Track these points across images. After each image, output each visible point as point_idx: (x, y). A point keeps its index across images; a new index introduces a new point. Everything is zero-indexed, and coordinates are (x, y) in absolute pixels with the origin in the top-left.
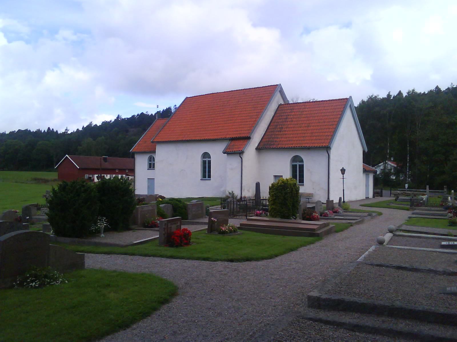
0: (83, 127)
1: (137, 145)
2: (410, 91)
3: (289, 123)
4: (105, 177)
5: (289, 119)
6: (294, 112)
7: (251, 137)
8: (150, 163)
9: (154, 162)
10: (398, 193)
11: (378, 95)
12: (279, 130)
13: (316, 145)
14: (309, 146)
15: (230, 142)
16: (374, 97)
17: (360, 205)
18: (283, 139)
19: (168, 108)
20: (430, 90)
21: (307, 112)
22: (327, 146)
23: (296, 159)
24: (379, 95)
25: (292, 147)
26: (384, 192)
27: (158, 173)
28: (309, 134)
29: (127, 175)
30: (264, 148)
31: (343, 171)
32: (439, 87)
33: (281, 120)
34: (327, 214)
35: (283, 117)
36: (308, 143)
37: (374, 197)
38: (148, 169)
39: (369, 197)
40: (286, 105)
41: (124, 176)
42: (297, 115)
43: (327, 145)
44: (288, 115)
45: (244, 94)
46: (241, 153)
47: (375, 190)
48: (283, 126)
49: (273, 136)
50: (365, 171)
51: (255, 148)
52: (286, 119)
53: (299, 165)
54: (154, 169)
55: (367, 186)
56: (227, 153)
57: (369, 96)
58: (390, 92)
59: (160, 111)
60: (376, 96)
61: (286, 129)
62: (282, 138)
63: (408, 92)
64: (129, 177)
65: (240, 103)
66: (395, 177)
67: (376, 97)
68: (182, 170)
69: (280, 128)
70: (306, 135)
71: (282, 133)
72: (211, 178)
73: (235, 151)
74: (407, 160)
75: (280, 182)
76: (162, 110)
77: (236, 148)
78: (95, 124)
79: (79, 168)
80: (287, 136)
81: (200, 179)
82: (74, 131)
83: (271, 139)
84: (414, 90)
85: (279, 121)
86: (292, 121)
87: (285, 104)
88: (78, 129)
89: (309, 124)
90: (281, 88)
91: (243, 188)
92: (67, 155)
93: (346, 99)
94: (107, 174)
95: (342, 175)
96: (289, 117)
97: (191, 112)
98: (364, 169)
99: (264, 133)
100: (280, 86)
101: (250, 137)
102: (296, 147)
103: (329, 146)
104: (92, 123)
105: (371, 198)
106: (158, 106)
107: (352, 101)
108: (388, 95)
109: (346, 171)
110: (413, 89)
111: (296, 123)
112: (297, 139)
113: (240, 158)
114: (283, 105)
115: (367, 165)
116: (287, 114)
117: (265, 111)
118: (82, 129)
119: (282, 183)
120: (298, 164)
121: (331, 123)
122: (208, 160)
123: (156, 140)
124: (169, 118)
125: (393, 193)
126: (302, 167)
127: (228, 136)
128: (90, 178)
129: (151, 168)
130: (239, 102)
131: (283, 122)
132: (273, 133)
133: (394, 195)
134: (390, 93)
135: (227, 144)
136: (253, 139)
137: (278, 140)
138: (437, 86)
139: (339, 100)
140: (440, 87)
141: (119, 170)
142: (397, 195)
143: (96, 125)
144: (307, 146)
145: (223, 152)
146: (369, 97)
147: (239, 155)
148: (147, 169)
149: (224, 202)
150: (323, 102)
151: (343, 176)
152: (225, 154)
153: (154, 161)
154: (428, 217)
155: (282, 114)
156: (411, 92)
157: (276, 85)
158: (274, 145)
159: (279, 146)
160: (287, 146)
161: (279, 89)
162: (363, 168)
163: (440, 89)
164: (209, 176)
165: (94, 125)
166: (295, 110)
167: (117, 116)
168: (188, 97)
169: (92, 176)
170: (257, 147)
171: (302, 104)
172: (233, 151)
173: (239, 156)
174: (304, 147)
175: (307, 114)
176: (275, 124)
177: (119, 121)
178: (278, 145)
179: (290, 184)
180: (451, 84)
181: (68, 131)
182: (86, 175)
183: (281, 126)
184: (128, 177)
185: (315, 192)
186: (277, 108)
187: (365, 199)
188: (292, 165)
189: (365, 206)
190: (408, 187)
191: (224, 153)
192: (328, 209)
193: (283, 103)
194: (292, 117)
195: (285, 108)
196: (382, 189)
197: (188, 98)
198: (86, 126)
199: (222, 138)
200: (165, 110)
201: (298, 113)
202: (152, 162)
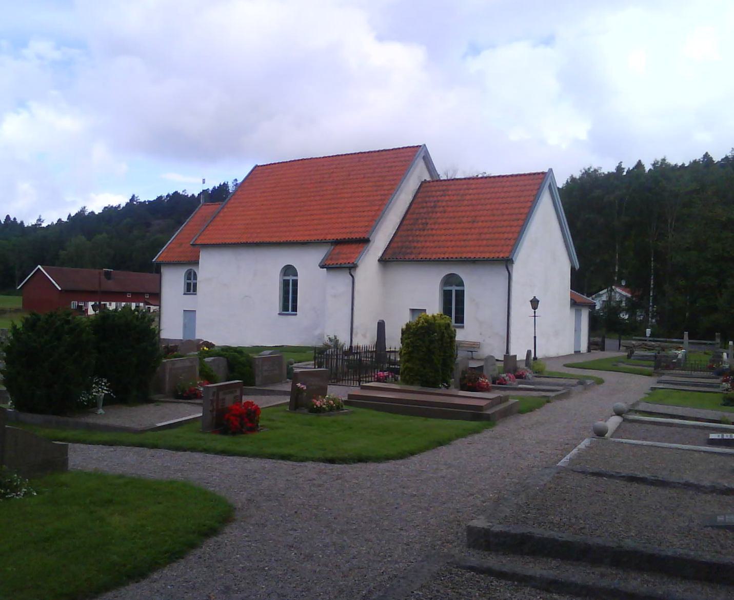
0: (70, 215)
1: (166, 250)
2: (658, 162)
3: (439, 215)
4: (108, 306)
5: (440, 207)
6: (449, 196)
7: (370, 239)
8: (188, 283)
9: (195, 281)
10: (633, 344)
12: (421, 226)
13: (487, 256)
14: (475, 258)
15: (333, 247)
16: (592, 172)
17: (565, 365)
18: (428, 244)
19: (222, 184)
20: (694, 159)
21: (472, 197)
22: (507, 257)
23: (450, 280)
24: (601, 168)
25: (443, 258)
26: (607, 341)
27: (201, 301)
28: (474, 236)
29: (146, 303)
30: (393, 259)
31: (535, 303)
32: (709, 155)
33: (425, 210)
34: (505, 380)
35: (429, 204)
36: (472, 252)
37: (589, 350)
38: (184, 294)
39: (580, 351)
40: (435, 183)
41: (142, 304)
42: (454, 201)
43: (506, 255)
44: (438, 201)
45: (359, 161)
46: (351, 268)
47: (592, 339)
48: (428, 220)
49: (411, 238)
50: (574, 304)
51: (378, 259)
52: (435, 207)
53: (456, 290)
54: (196, 294)
55: (577, 330)
56: (326, 266)
57: (584, 169)
58: (621, 162)
59: (208, 189)
61: (433, 226)
62: (426, 241)
64: (151, 306)
65: (351, 177)
66: (627, 315)
67: (596, 171)
68: (247, 296)
69: (423, 224)
70: (469, 237)
71: (425, 232)
72: (297, 311)
73: (341, 264)
74: (650, 286)
75: (421, 322)
76: (211, 188)
77: (343, 259)
78: (90, 211)
79: (60, 289)
80: (435, 238)
81: (278, 313)
82: (53, 223)
83: (407, 243)
84: (664, 160)
85: (421, 210)
86: (445, 212)
87: (433, 181)
88: (60, 220)
89: (476, 217)
90: (427, 152)
91: (354, 331)
92: (39, 266)
93: (543, 173)
94: (111, 301)
95: (533, 310)
96: (440, 204)
97: (264, 192)
98: (572, 301)
99: (394, 232)
100: (424, 149)
101: (369, 238)
102: (452, 258)
103: (510, 257)
104: (86, 208)
105: (584, 352)
106: (204, 180)
107: (553, 178)
108: (618, 167)
109: (540, 303)
110: (663, 158)
111: (451, 215)
112: (453, 243)
113: (350, 276)
114: (429, 182)
115: (577, 293)
116: (435, 199)
117: (396, 193)
118: (68, 219)
119: (425, 322)
120: (454, 289)
121: (514, 217)
122: (292, 280)
123: (199, 242)
124: (224, 203)
126: (460, 295)
127: (329, 237)
128: (80, 307)
129: (190, 291)
130: (349, 175)
131: (428, 213)
132: (409, 233)
133: (625, 348)
134: (622, 164)
135: (327, 253)
136: (374, 242)
137: (419, 245)
138: (707, 153)
139: (530, 174)
140: (711, 156)
141: (133, 294)
142: (631, 347)
143: (92, 213)
144: (470, 258)
145: (319, 266)
146: (583, 171)
147: (348, 271)
148: (183, 293)
149: (320, 355)
150: (501, 179)
151: (535, 312)
152: (323, 268)
153: (196, 280)
154: (686, 388)
155: (427, 199)
156: (659, 163)
157: (417, 146)
158: (411, 253)
159: (421, 256)
160: (434, 256)
161: (422, 154)
162: (571, 299)
163: (711, 158)
164: (295, 309)
165: (89, 213)
166: (450, 193)
167: (130, 198)
168: (259, 165)
169: (83, 305)
170: (381, 257)
171: (464, 181)
172: (337, 264)
173: (349, 274)
174: (466, 259)
175: (472, 200)
176: (415, 216)
177: (134, 207)
178: (419, 254)
179: (440, 326)
180: (731, 149)
181: (42, 222)
182: (72, 302)
183: (424, 221)
184: (148, 308)
185: (484, 341)
186: (419, 188)
187: (571, 355)
188: (444, 291)
189: (573, 367)
190: (650, 334)
191: (322, 267)
192: (506, 370)
193: (428, 179)
194: (444, 204)
195: (433, 189)
196: (604, 338)
197: (259, 166)
198: (75, 213)
199: (318, 240)
200: (216, 188)
201: (455, 198)
202: (192, 282)
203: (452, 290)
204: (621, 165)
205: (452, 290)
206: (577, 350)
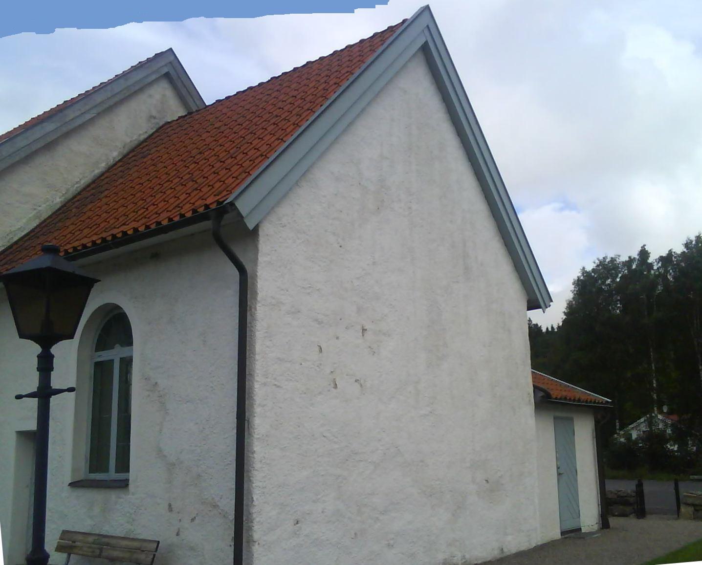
2: (691, 242)
11: (616, 255)
24: (619, 256)
37: (604, 524)
58: (644, 245)
60: (613, 256)
63: (685, 242)
67: (613, 260)
110: (698, 235)
125: (690, 501)
146: (597, 262)
156: (694, 243)
162: (536, 388)
196: (640, 485)
203: (112, 361)
204: (645, 249)
205: (112, 361)
206: (570, 526)
